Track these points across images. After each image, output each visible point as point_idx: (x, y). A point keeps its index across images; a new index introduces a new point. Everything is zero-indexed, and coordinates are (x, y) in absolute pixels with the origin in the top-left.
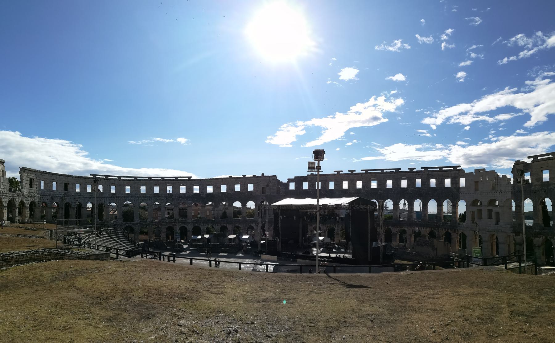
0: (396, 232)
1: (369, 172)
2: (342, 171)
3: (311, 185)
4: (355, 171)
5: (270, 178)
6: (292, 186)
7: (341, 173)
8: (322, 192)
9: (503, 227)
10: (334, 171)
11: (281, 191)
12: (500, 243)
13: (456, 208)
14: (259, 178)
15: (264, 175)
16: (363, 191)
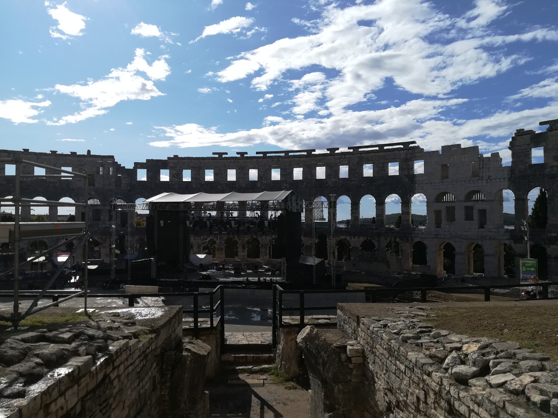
0: (311, 244)
1: (268, 155)
2: (226, 154)
3: (175, 175)
4: (246, 153)
5: (104, 159)
6: (142, 176)
7: (224, 156)
8: (194, 186)
9: (493, 232)
10: (214, 154)
11: (122, 182)
12: (487, 255)
13: (409, 207)
14: (82, 158)
15: (92, 154)
16: (259, 184)
